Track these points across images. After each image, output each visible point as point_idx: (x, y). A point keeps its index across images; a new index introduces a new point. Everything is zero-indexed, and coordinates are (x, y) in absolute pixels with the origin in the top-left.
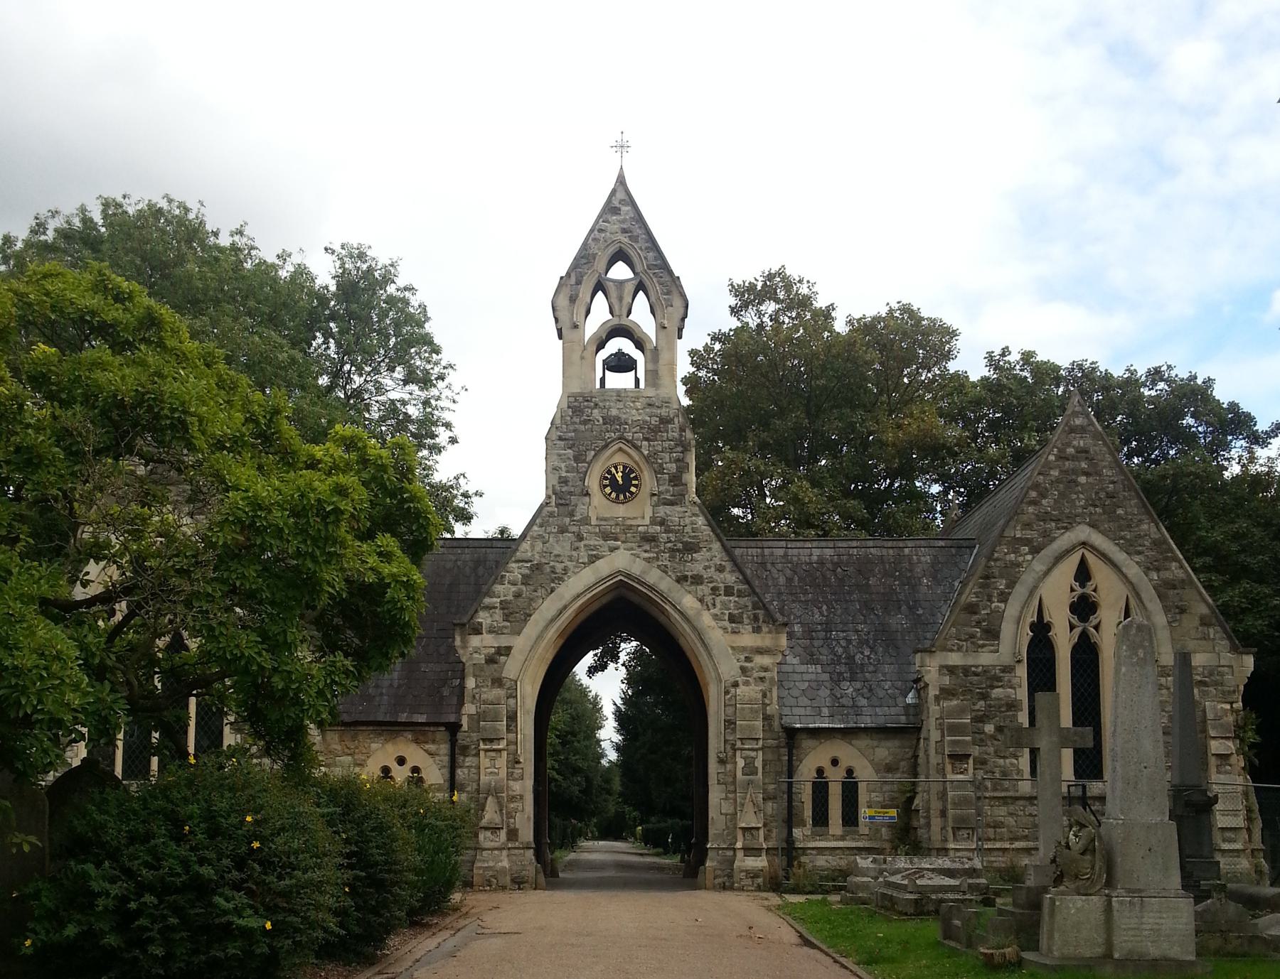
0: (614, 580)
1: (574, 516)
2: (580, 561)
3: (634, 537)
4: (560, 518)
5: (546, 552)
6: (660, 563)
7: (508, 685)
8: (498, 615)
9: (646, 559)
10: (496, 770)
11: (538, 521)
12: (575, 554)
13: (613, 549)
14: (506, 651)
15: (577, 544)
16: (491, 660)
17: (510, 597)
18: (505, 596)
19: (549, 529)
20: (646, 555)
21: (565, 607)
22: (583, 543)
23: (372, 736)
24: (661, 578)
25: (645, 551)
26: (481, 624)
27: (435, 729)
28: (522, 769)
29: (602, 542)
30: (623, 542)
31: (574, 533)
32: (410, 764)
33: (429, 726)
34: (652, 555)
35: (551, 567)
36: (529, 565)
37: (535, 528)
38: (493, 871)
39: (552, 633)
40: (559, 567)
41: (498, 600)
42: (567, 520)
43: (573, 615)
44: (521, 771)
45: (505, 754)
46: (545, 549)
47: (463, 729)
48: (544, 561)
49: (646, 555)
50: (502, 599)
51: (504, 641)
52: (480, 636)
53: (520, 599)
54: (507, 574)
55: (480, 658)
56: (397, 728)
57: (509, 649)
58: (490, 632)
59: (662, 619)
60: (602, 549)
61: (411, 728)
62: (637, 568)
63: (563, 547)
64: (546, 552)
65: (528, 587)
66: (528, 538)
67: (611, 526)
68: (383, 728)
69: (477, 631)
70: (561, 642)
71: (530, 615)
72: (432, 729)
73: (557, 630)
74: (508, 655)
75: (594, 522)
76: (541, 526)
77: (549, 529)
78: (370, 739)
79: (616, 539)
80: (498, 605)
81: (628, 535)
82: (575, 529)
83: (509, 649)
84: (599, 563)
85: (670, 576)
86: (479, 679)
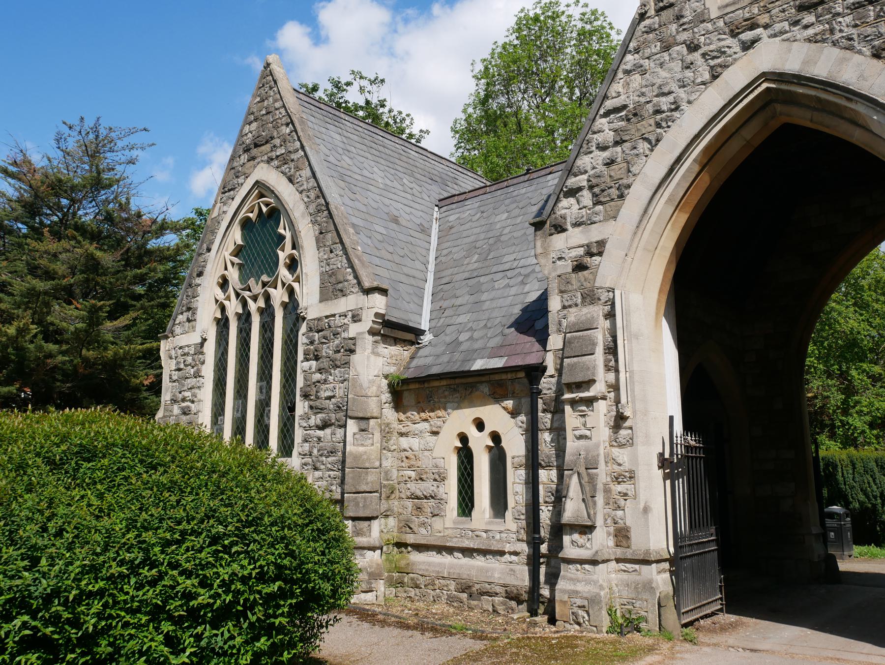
0: (756, 92)
1: (682, 17)
2: (699, 80)
3: (784, 11)
4: (664, 29)
5: (646, 86)
6: (838, 35)
7: (604, 296)
8: (586, 197)
9: (809, 40)
10: (588, 433)
11: (632, 45)
12: (689, 74)
13: (747, 46)
14: (597, 249)
15: (690, 58)
16: (579, 267)
17: (601, 168)
18: (594, 168)
19: (648, 51)
20: (810, 32)
21: (678, 160)
22: (700, 51)
23: (446, 393)
24: (844, 60)
25: (806, 27)
26: (564, 217)
27: (513, 375)
28: (631, 428)
29: (730, 41)
30: (766, 27)
31: (684, 42)
32: (488, 429)
33: (507, 372)
34: (819, 28)
35: (654, 105)
36: (623, 113)
37: (629, 57)
38: (581, 598)
39: (662, 206)
40: (665, 103)
41: (585, 177)
42: (674, 27)
43: (697, 168)
44: (630, 431)
45: (601, 406)
46: (644, 83)
47: (548, 373)
48: (643, 100)
49: (810, 32)
50: (591, 173)
51: (594, 234)
52: (563, 235)
53: (614, 167)
54: (595, 136)
55: (566, 266)
56: (470, 380)
57: (601, 244)
58: (576, 225)
59: (857, 136)
60: (732, 50)
61: (483, 379)
62: (792, 65)
63: (670, 70)
64: (646, 86)
65: (625, 144)
66: (620, 74)
67: (744, 8)
68: (458, 381)
69: (560, 229)
70: (682, 218)
71: (628, 187)
72: (509, 376)
73: (669, 200)
74: (600, 254)
75: (714, 14)
76: (637, 51)
77: (648, 51)
78: (445, 397)
79: (753, 27)
80: (585, 183)
81: (773, 12)
82: (684, 36)
83: (601, 244)
84: (726, 74)
85: (860, 52)
86: (565, 296)
